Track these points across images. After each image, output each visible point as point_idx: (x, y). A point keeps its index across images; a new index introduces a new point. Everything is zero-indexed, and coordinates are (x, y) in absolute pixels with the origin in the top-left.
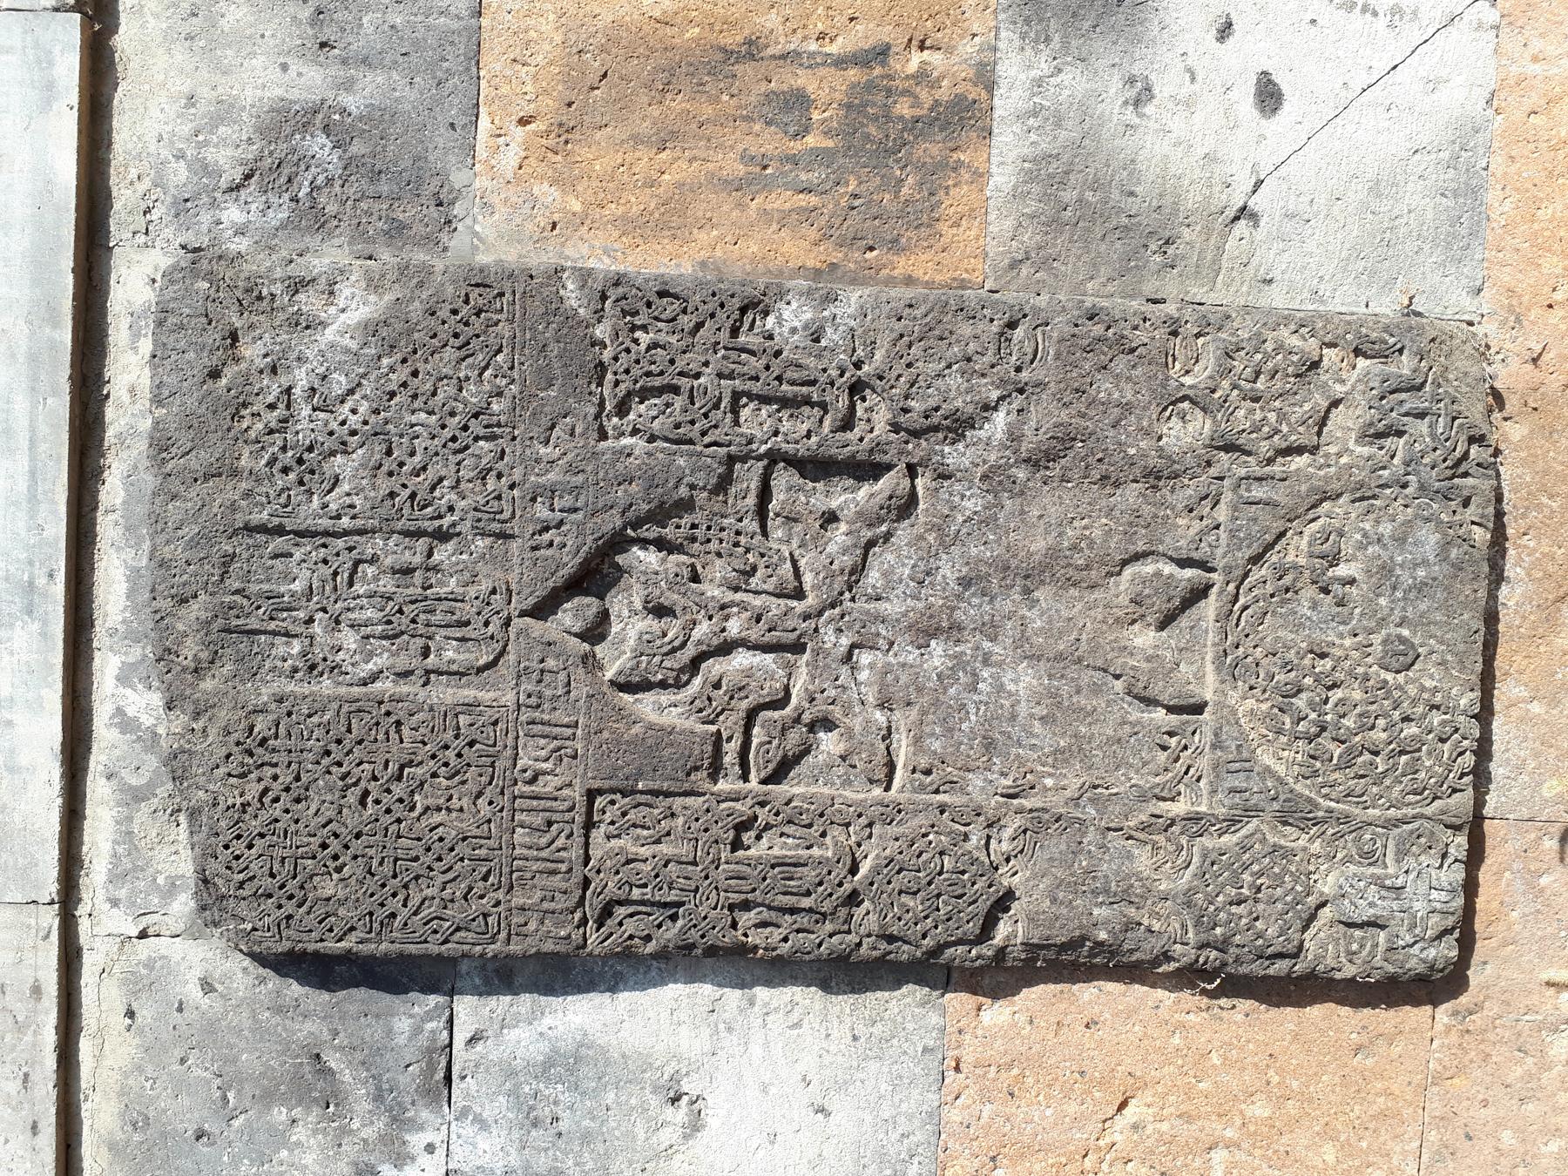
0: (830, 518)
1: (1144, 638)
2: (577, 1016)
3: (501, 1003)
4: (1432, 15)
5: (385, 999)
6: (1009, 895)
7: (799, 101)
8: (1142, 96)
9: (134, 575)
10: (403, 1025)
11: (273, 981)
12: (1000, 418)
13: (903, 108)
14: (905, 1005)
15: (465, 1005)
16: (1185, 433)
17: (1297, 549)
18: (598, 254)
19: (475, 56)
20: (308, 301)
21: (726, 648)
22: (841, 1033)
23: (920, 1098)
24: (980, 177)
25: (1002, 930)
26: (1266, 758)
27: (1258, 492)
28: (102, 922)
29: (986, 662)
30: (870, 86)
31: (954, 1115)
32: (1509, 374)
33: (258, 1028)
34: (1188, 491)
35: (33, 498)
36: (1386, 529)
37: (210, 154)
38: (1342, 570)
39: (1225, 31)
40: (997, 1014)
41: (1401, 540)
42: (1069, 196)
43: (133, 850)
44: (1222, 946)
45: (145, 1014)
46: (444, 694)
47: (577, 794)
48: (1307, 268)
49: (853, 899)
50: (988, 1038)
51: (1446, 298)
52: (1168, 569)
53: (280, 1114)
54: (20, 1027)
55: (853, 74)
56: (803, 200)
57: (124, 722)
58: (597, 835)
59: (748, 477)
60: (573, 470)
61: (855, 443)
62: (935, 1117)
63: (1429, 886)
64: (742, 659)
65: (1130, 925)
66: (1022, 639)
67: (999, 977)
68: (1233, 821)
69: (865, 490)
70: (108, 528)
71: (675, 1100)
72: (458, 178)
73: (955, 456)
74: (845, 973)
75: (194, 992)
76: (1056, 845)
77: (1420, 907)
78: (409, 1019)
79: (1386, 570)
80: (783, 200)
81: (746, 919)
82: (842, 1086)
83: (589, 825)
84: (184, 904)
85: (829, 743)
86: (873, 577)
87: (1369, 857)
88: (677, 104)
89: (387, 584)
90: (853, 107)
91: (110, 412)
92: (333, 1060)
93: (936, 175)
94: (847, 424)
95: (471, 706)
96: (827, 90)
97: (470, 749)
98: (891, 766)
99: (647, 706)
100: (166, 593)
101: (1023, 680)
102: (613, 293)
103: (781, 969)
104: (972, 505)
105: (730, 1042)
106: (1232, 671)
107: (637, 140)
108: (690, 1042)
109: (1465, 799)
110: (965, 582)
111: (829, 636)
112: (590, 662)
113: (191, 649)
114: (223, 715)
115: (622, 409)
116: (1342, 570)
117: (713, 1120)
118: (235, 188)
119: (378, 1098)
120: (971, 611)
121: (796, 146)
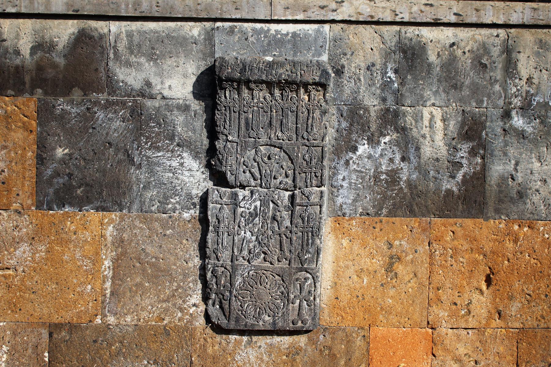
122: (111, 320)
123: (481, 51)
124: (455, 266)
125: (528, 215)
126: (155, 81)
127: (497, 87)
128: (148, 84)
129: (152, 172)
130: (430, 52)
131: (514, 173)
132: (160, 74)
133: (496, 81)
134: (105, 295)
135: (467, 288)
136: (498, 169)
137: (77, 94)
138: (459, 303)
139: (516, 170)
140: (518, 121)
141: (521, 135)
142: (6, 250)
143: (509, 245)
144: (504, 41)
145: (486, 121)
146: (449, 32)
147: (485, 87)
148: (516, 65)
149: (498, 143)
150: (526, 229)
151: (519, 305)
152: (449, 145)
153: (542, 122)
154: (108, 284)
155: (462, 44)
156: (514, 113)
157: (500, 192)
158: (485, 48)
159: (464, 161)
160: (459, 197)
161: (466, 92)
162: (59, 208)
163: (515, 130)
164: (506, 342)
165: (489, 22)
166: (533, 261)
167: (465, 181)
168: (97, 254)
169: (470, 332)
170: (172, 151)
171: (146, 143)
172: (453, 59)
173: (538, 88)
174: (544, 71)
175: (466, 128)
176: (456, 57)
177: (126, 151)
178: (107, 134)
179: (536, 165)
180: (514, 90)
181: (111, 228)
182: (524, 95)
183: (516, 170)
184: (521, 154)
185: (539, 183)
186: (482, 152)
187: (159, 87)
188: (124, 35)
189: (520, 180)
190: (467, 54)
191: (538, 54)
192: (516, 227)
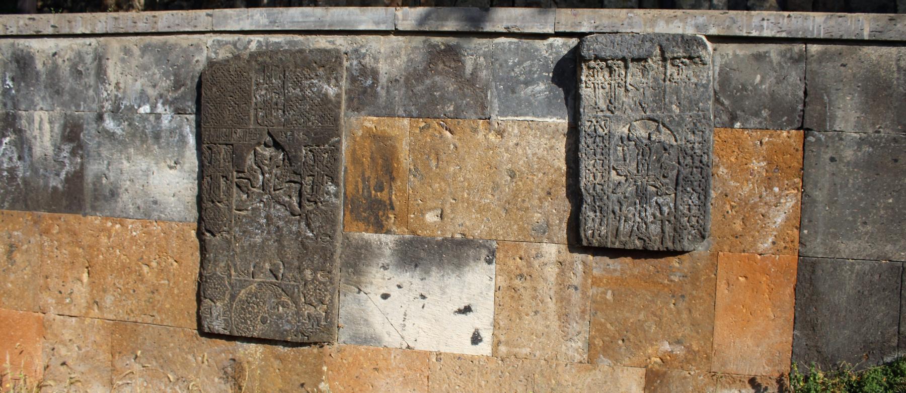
0: (290, 197)
1: (267, 266)
2: (192, 140)
3: (194, 124)
4: (404, 334)
5: (195, 99)
6: (214, 236)
7: (382, 190)
8: (385, 267)
9: (279, 43)
10: (190, 104)
11: (198, 75)
12: (311, 234)
13: (381, 213)
14: (195, 213)
15: (193, 117)
16: (308, 274)
17: (284, 298)
18: (344, 146)
19: (389, 116)
20: (333, 81)
21: (263, 174)
22: (189, 199)
23: (176, 216)
24: (367, 231)
25: (208, 234)
26: (243, 291)
27: (296, 290)
28: (209, 39)
29: (262, 232)
30: (385, 206)
31: (173, 224)
32: (326, 347)
33: (188, 73)
34: (298, 276)
35: (294, 22)
36: (290, 318)
37: (367, 59)
38: (281, 308)
39: (399, 287)
40: (193, 233)
41: (288, 321)
42: (363, 251)
43: (224, 45)
44: (206, 282)
45: (191, 48)
46: (252, 113)
47: (232, 142)
48: (347, 305)
49: (213, 202)
50: (189, 232)
51: (343, 336)
52: (282, 271)
53: (172, 78)
54: (188, 23)
55: (388, 202)
56: (361, 190)
57: (249, 42)
58: (225, 146)
59: (297, 178)
60: (297, 140)
61: (305, 203)
62: (173, 220)
63: (218, 326)
64: (261, 177)
65: (209, 261)
66: (267, 240)
67: (200, 234)
68: (230, 284)
69: (295, 204)
70: (289, 37)
71: (175, 163)
72: (363, 112)
73: (303, 224)
74: (200, 199)
75: (196, 59)
76: (225, 245)
77: (214, 323)
78: (191, 105)
79: (281, 318)
80: (360, 186)
81: (209, 178)
82: (179, 200)
83: (227, 145)
84: (213, 56)
85: (245, 196)
86: (278, 207)
87: (224, 313)
88: (380, 161)
89: (274, 100)
90: (380, 202)
91: (314, 36)
92: (183, 89)
93: (366, 221)
94: (309, 201)
95: (249, 119)
96: (383, 196)
97: (240, 121)
98: (240, 210)
99: (251, 156)
100: (274, 52)
101: (258, 239)
102: (336, 148)
103: (200, 185)
104: (294, 228)
105: (187, 175)
106: (260, 284)
107: (372, 153)
108: (187, 166)
109: (236, 334)
110: (278, 227)
111: (266, 197)
112: (259, 144)
113: (260, 59)
114: (247, 67)
115: (310, 151)
116: (281, 308)
117: (172, 171)
118: (360, 63)
119: (176, 99)
120: (272, 228)
121: (372, 188)
123: (77, 59)
124: (59, 258)
125: (119, 213)
127: (91, 92)
130: (37, 62)
131: (107, 172)
133: (90, 86)
135: (70, 279)
136: (93, 168)
138: (63, 291)
139: (108, 169)
140: (109, 124)
141: (111, 135)
143: (104, 240)
144: (96, 49)
145: (82, 124)
146: (51, 42)
147: (82, 92)
148: (105, 71)
149: (92, 145)
150: (118, 226)
151: (113, 298)
152: (55, 145)
153: (130, 125)
155: (62, 53)
156: (106, 116)
157: (95, 190)
158: (80, 56)
159: (67, 161)
160: (63, 193)
161: (66, 97)
163: (107, 132)
164: (102, 332)
165: (79, 32)
166: (123, 257)
167: (67, 180)
169: (74, 319)
172: (56, 67)
173: (124, 92)
174: (129, 76)
175: (68, 130)
176: (57, 66)
179: (126, 164)
180: (105, 94)
182: (113, 99)
183: (108, 169)
184: (112, 155)
185: (128, 183)
186: (81, 152)
189: (112, 179)
190: (67, 62)
191: (123, 60)
192: (109, 224)
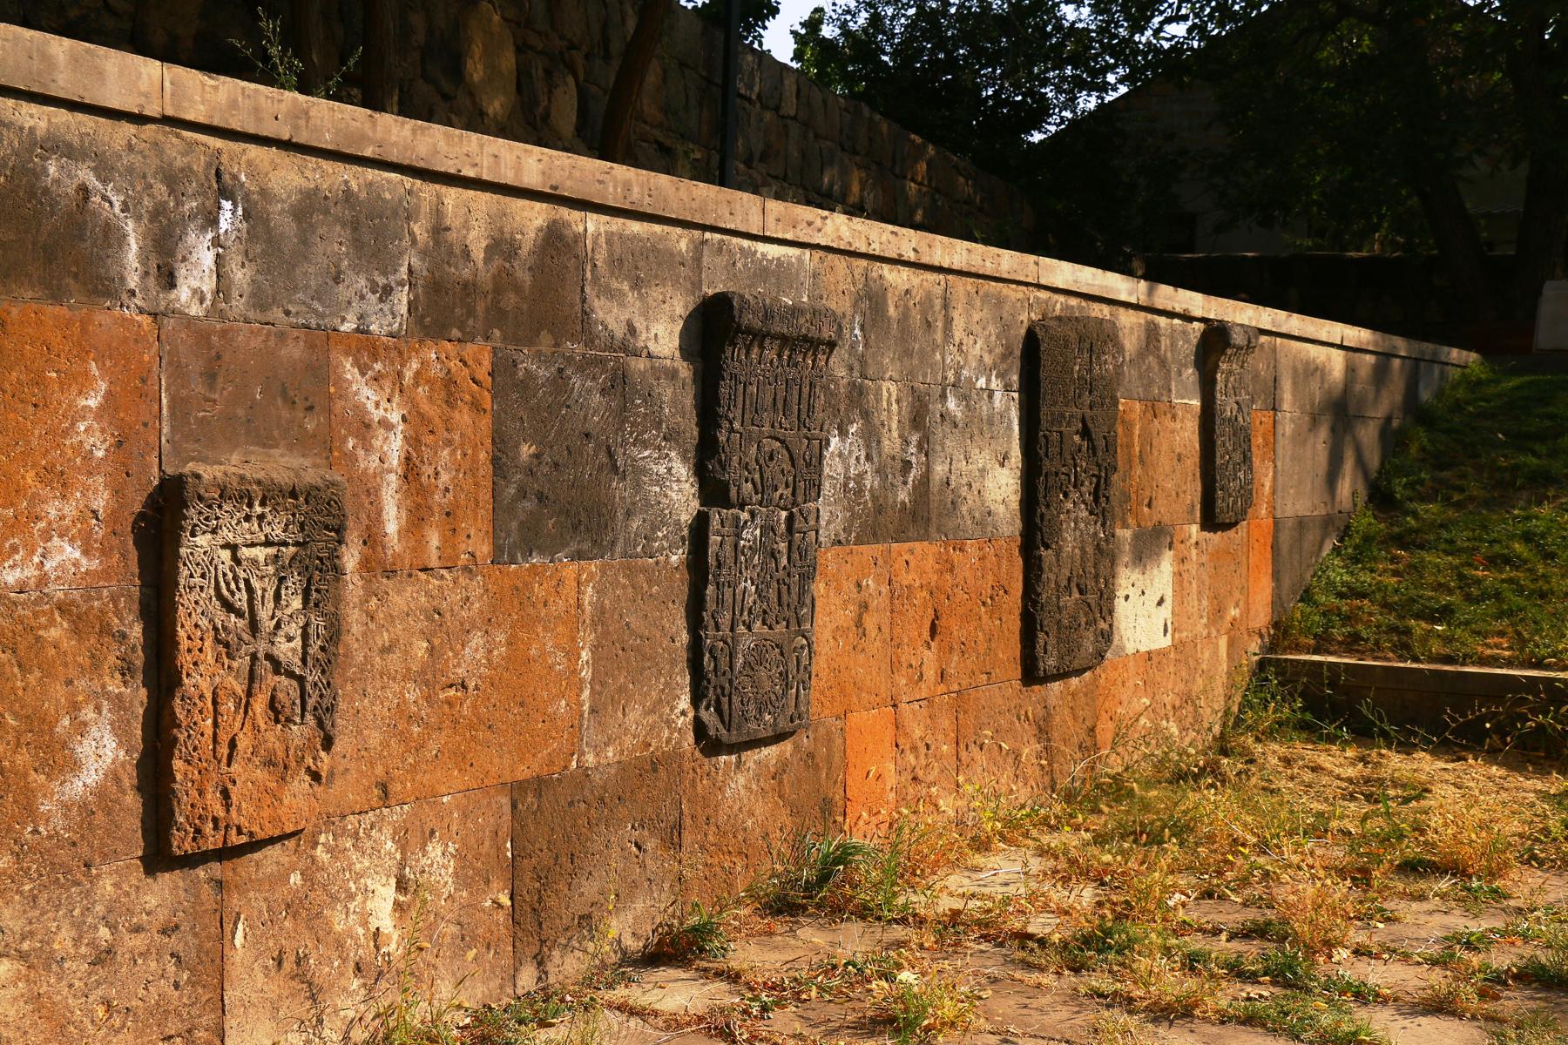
122: (590, 759)
126: (639, 324)
128: (632, 330)
129: (638, 486)
132: (645, 314)
134: (582, 715)
137: (545, 341)
142: (451, 649)
154: (586, 693)
162: (525, 560)
168: (573, 639)
170: (659, 448)
171: (631, 433)
177: (608, 448)
178: (585, 418)
181: (590, 589)
187: (644, 336)
188: (602, 240)
